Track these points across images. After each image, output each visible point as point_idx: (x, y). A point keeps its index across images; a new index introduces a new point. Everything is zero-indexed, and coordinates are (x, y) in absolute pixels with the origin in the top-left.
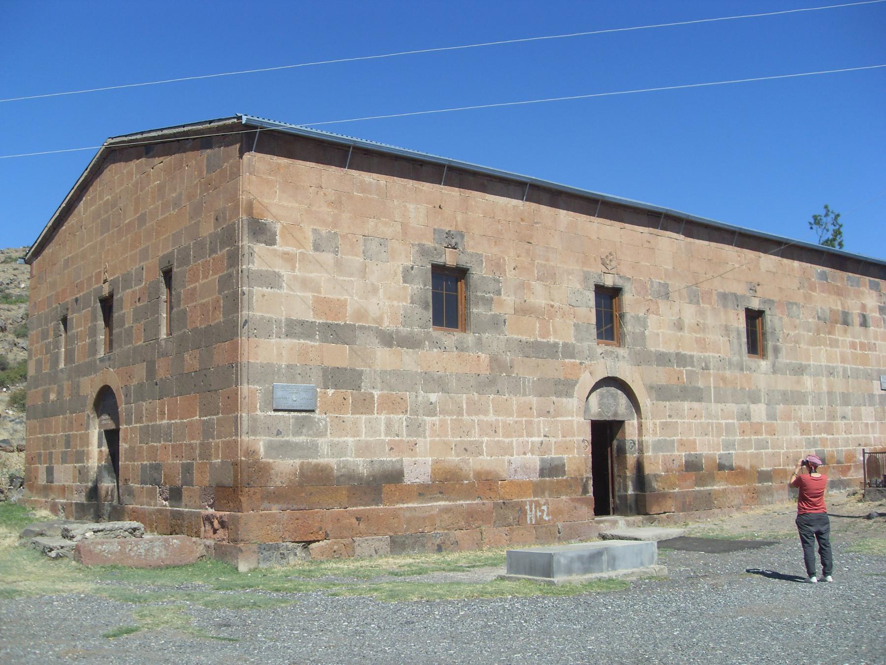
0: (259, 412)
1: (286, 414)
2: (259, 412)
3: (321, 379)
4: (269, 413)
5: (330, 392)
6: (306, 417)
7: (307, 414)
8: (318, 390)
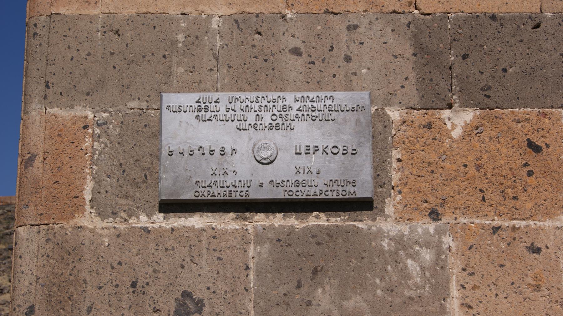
0: (89, 220)
1: (227, 222)
2: (89, 220)
3: (406, 68)
4: (143, 220)
5: (459, 120)
6: (330, 233)
7: (337, 220)
8: (394, 114)
